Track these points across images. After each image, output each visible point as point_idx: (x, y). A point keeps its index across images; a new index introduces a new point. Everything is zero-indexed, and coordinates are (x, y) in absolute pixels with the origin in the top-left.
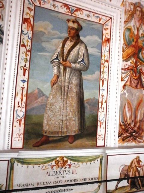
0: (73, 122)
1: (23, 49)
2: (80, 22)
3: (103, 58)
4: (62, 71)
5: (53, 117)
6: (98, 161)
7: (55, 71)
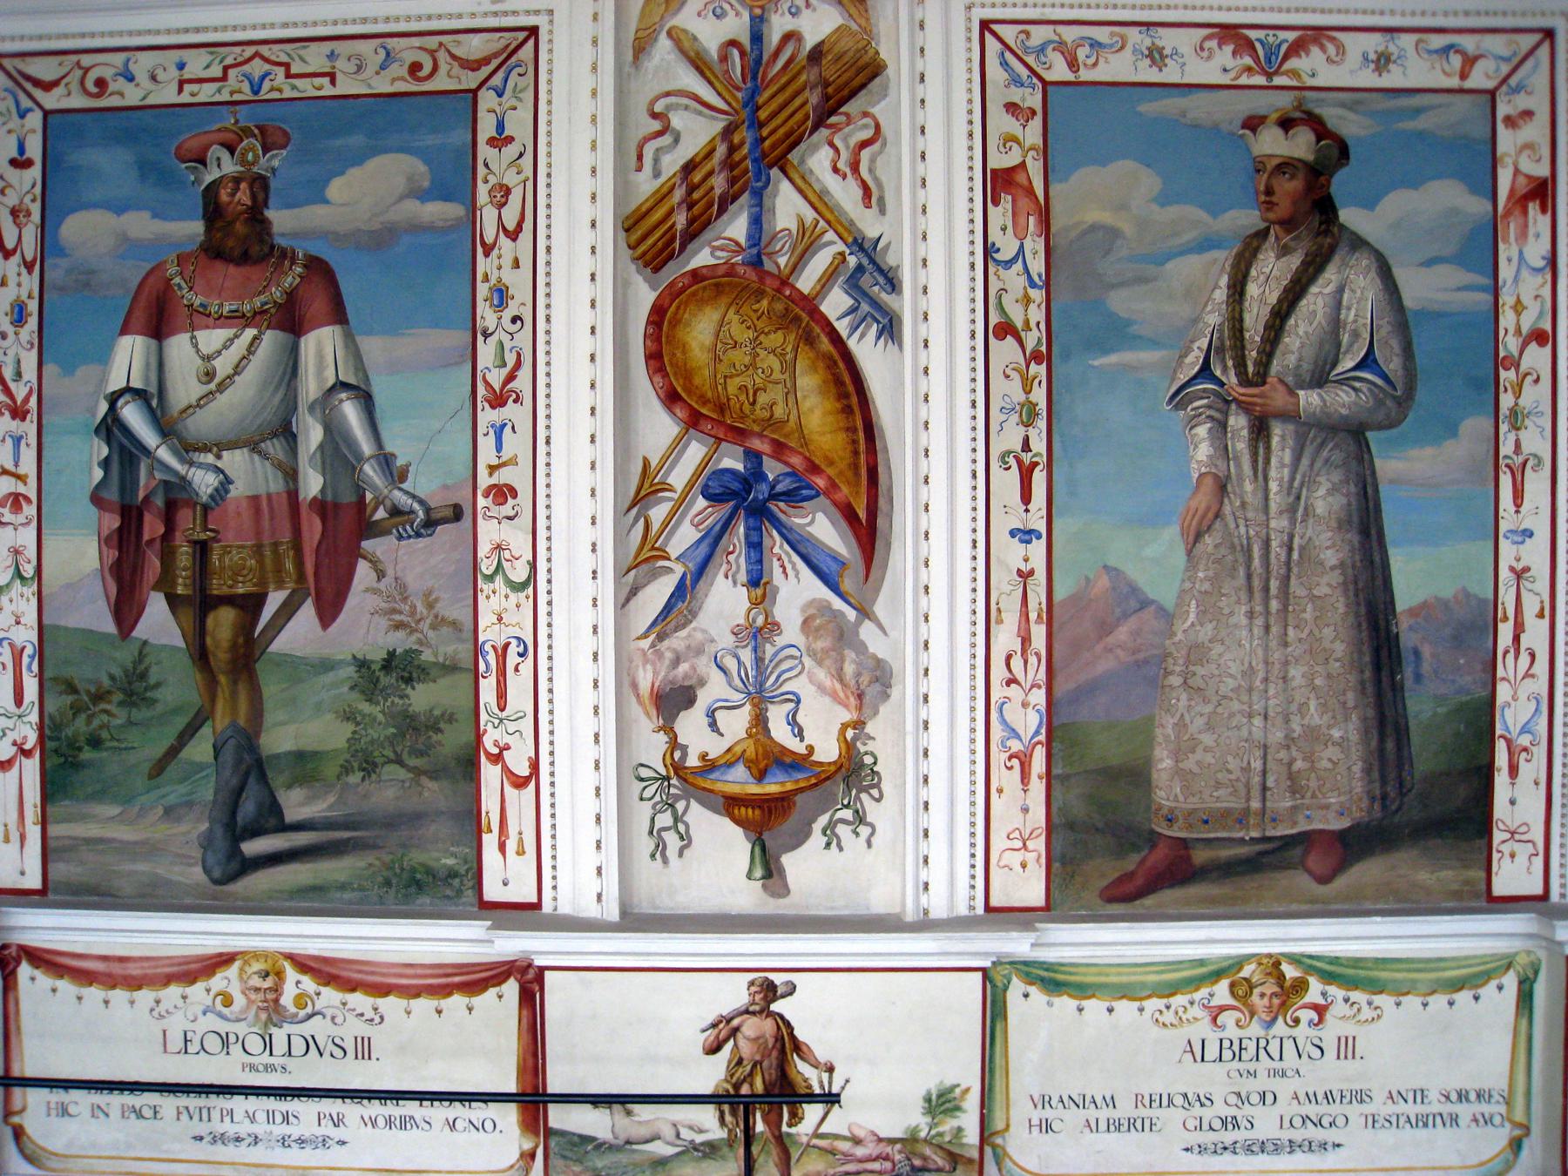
0: (1332, 752)
1: (1006, 351)
2: (1333, 116)
3: (1507, 320)
4: (1241, 446)
5: (1210, 727)
6: (1500, 988)
7: (1204, 451)
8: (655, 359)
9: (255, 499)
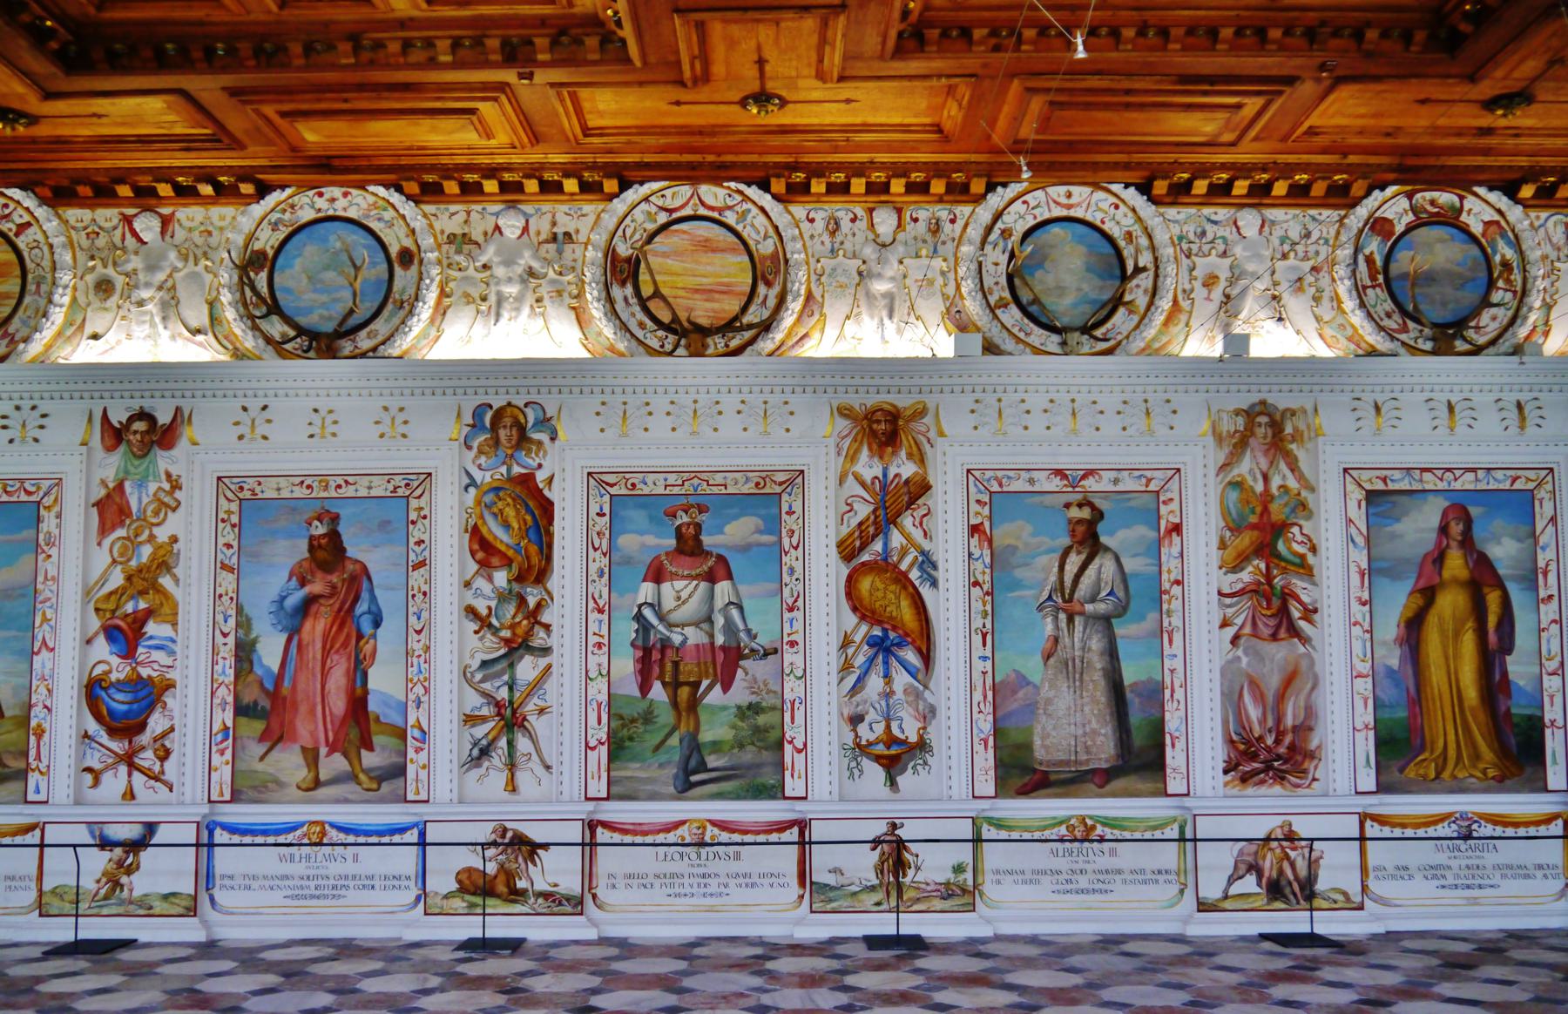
0: (1102, 738)
1: (976, 591)
2: (1098, 502)
3: (1165, 576)
5: (1054, 728)
7: (1049, 628)
8: (849, 595)
9: (697, 646)
